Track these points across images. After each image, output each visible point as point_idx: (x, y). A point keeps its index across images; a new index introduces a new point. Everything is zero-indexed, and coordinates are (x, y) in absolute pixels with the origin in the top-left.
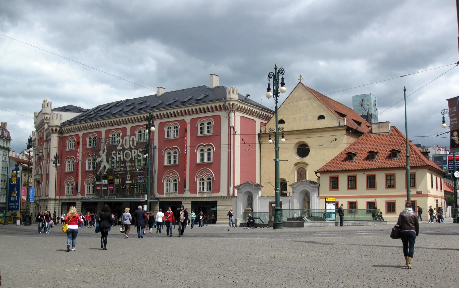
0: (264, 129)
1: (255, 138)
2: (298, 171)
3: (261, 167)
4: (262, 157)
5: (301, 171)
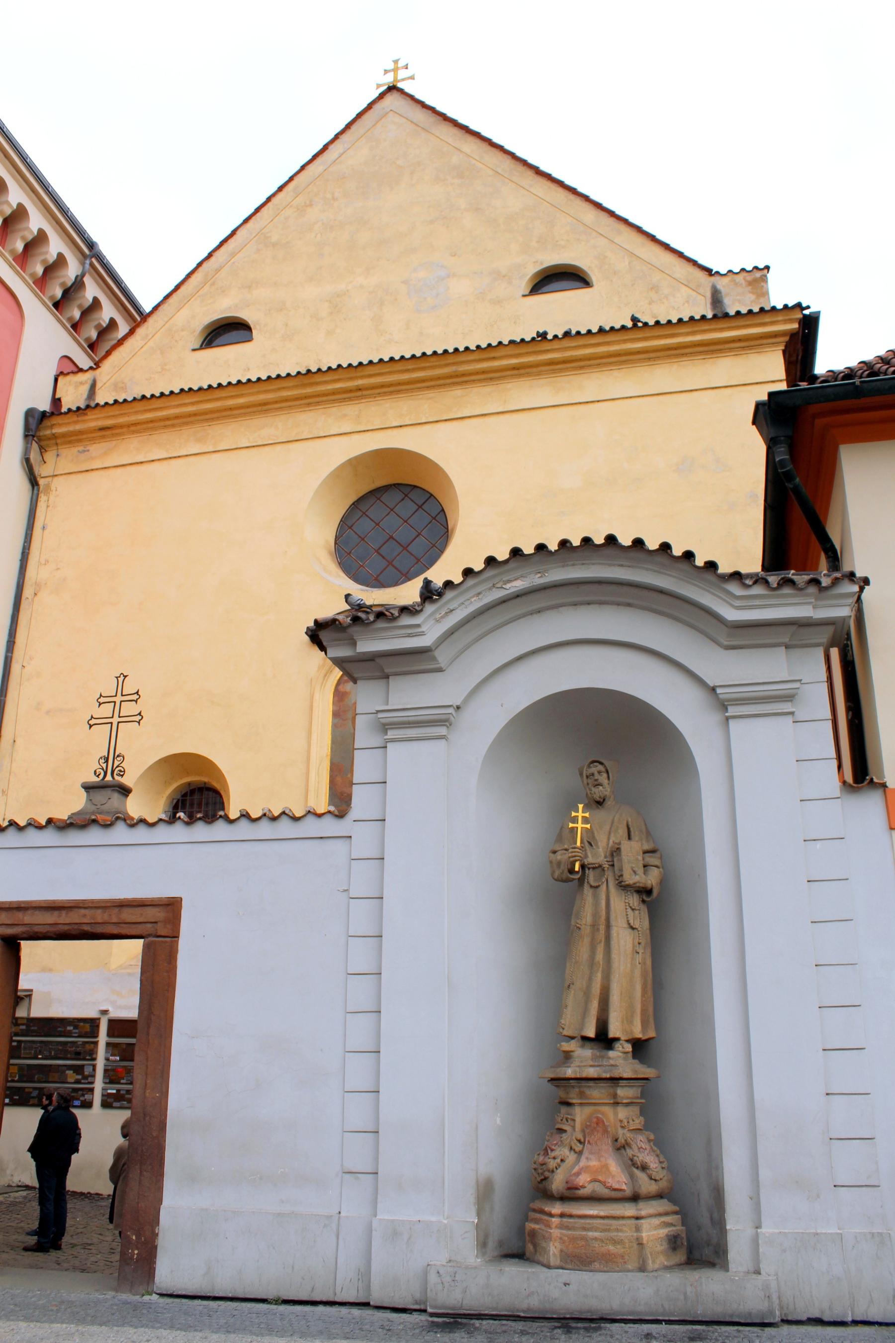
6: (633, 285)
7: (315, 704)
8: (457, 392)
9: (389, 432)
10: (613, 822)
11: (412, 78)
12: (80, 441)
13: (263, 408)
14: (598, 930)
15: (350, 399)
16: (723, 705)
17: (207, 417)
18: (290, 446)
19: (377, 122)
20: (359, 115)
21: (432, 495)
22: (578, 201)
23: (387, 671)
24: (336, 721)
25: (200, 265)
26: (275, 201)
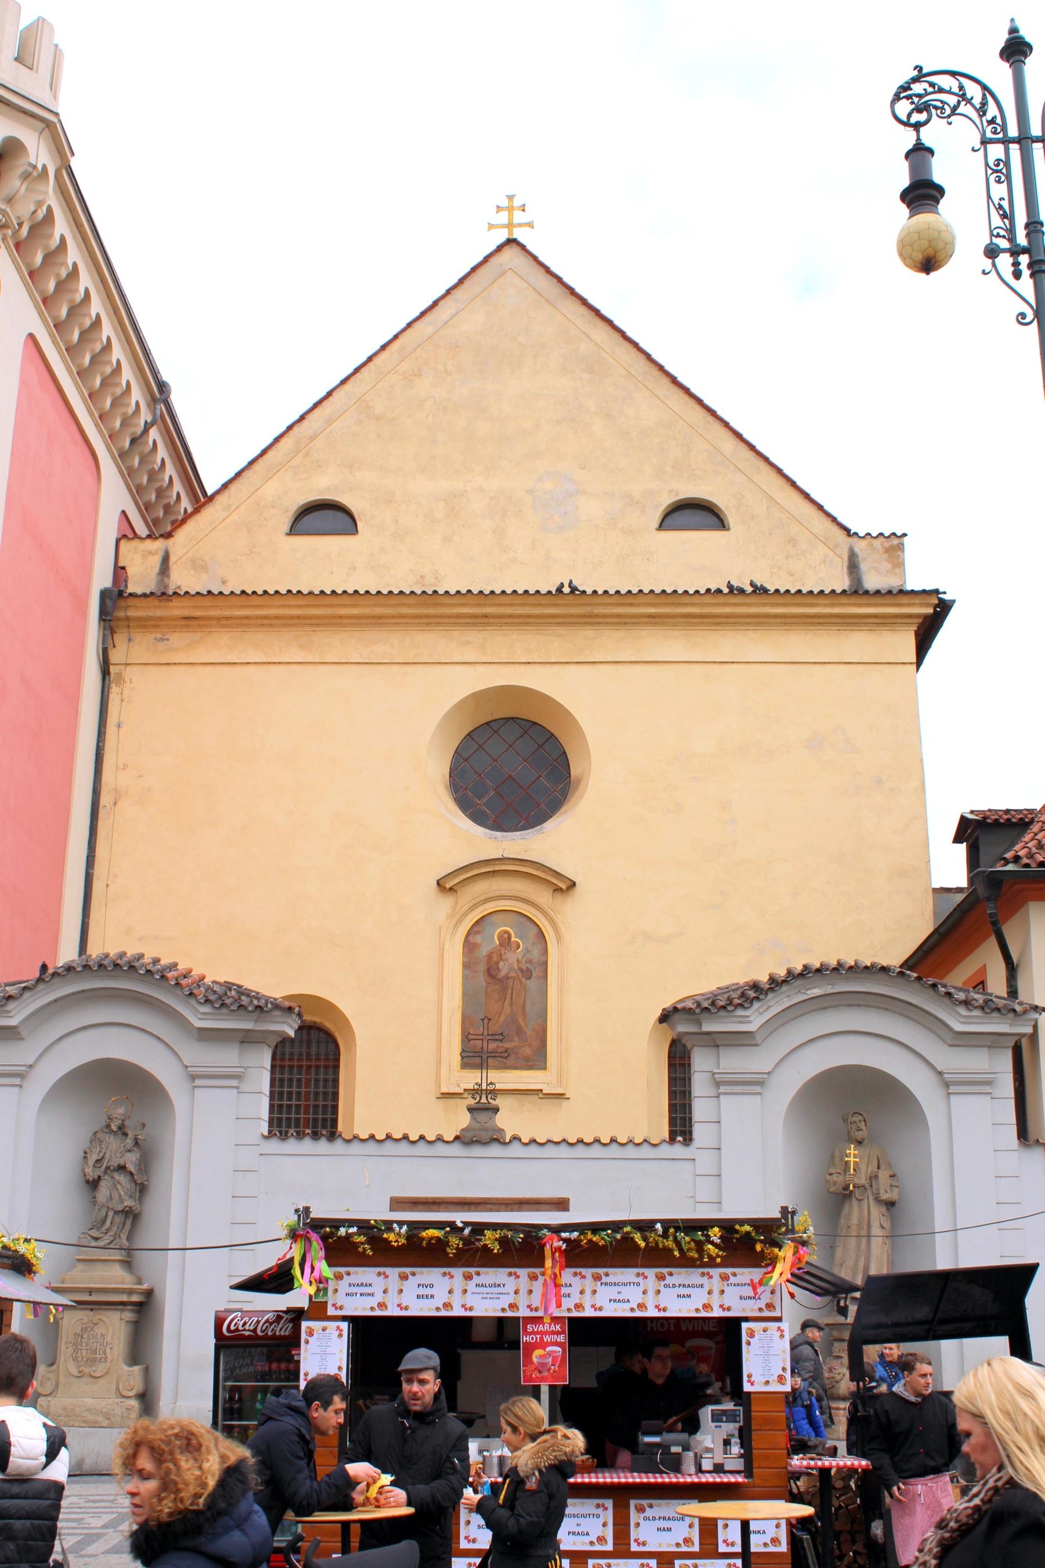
0: (156, 561)
1: (84, 613)
2: (478, 939)
3: (97, 886)
4: (118, 796)
5: (506, 941)
6: (770, 534)
7: (446, 955)
8: (589, 632)
9: (517, 666)
10: (869, 1156)
11: (530, 225)
12: (156, 626)
13: (377, 621)
14: (863, 1229)
15: (474, 624)
16: (947, 1085)
17: (313, 622)
18: (408, 668)
19: (494, 281)
20: (474, 269)
21: (553, 735)
22: (717, 426)
23: (718, 1043)
24: (467, 972)
25: (290, 428)
26: (376, 361)
